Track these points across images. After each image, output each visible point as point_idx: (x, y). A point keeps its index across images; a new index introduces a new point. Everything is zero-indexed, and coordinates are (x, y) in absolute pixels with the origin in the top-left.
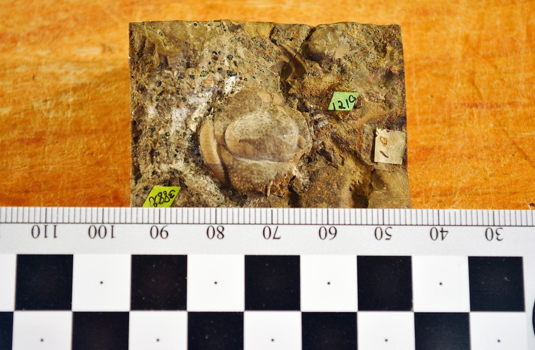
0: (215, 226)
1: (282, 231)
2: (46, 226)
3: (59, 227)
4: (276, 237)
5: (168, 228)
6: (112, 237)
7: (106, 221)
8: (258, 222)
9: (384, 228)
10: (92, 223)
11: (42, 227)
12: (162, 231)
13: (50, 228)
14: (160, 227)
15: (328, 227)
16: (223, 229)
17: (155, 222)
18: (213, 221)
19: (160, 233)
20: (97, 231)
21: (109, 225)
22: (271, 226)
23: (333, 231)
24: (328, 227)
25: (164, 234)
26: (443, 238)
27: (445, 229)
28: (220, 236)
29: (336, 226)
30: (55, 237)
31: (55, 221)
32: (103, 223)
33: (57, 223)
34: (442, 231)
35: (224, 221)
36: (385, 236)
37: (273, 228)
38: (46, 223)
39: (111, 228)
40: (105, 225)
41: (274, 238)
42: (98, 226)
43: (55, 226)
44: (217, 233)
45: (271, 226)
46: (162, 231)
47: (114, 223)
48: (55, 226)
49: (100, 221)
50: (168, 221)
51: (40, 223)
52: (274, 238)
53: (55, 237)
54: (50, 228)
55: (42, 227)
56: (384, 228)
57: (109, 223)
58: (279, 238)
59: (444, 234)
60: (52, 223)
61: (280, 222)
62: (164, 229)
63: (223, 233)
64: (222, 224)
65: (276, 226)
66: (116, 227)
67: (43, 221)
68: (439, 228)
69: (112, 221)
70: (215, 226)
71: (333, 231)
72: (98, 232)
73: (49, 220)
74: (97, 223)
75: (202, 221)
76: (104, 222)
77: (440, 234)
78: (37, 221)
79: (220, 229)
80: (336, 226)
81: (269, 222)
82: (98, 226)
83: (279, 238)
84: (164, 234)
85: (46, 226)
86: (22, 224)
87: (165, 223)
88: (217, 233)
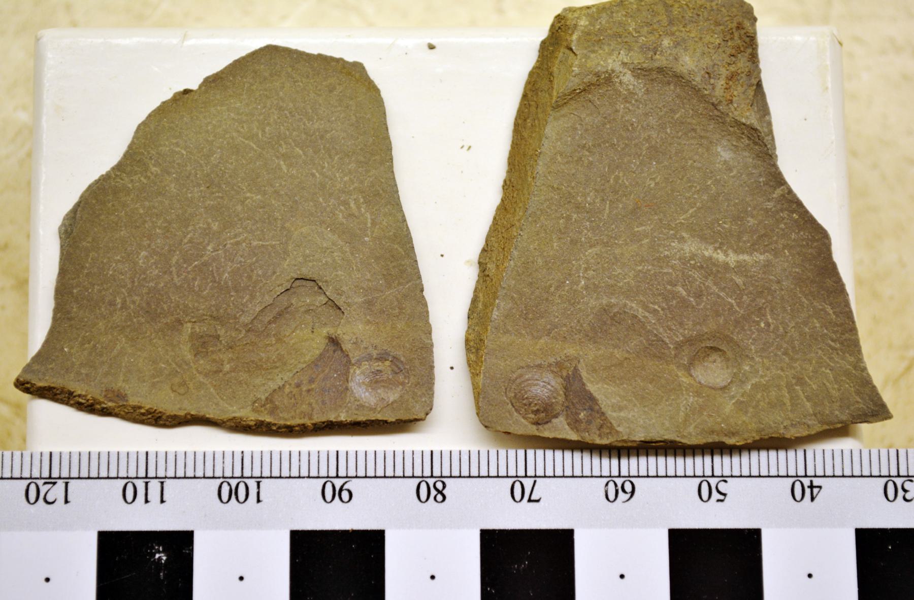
0: (431, 481)
1: (543, 488)
2: (147, 483)
3: (168, 483)
4: (532, 498)
5: (352, 485)
6: (259, 501)
7: (247, 473)
8: (503, 473)
9: (713, 482)
10: (224, 477)
11: (140, 484)
12: (341, 490)
13: (154, 486)
14: (338, 483)
16: (444, 487)
17: (330, 475)
18: (427, 473)
19: (338, 493)
21: (254, 480)
22: (524, 480)
23: (628, 487)
24: (619, 481)
25: (345, 495)
26: (813, 499)
27: (816, 482)
28: (440, 498)
29: (632, 479)
30: (162, 501)
31: (161, 474)
32: (242, 477)
33: (166, 477)
34: (812, 487)
35: (446, 473)
36: (716, 496)
37: (528, 483)
38: (146, 477)
39: (256, 484)
40: (246, 481)
41: (530, 500)
43: (162, 483)
44: (433, 492)
45: (524, 480)
46: (341, 490)
47: (261, 477)
48: (162, 483)
49: (238, 473)
50: (352, 473)
51: (137, 478)
52: (530, 500)
53: (162, 501)
54: (154, 486)
55: (140, 484)
56: (713, 482)
57: (252, 477)
58: (538, 501)
59: (815, 490)
60: (156, 478)
61: (540, 472)
62: (345, 487)
63: (444, 492)
64: (441, 477)
65: (532, 480)
66: (265, 483)
67: (142, 474)
68: (806, 482)
69: (257, 473)
70: (431, 481)
71: (628, 487)
72: (234, 493)
73: (151, 474)
74: (232, 477)
75: (408, 473)
76: (245, 475)
77: (808, 491)
78: (132, 474)
79: (439, 486)
80: (632, 479)
81: (521, 473)
82: (234, 483)
83: (538, 501)
84: (345, 495)
85: (147, 483)
86: (203, 480)
87: (347, 477)
88: (433, 492)
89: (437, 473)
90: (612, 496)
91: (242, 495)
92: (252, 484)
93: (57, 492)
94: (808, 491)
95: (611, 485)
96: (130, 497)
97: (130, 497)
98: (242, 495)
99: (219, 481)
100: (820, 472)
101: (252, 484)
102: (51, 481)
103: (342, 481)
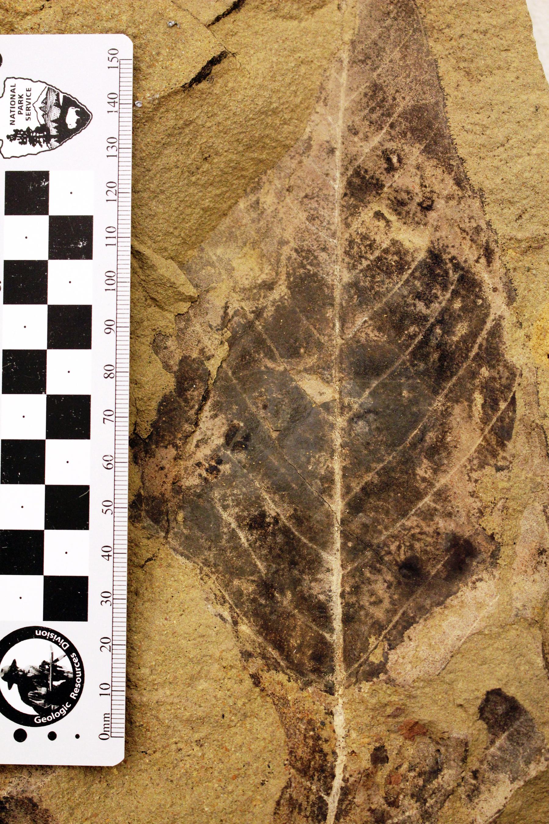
0: (114, 372)
1: (110, 425)
5: (113, 334)
7: (119, 284)
9: (112, 508)
11: (115, 234)
13: (114, 241)
14: (114, 327)
15: (113, 462)
19: (109, 327)
20: (111, 277)
22: (114, 416)
23: (110, 466)
24: (113, 462)
25: (108, 331)
28: (106, 376)
36: (105, 509)
37: (112, 418)
42: (115, 278)
44: (109, 373)
45: (114, 416)
54: (114, 241)
55: (115, 234)
56: (112, 508)
59: (107, 558)
67: (120, 235)
68: (111, 553)
69: (119, 289)
70: (114, 372)
71: (110, 466)
77: (107, 554)
79: (112, 376)
82: (115, 278)
84: (108, 331)
88: (109, 373)
89: (118, 374)
90: (106, 458)
91: (108, 282)
92: (114, 287)
93: (112, 196)
94: (107, 554)
95: (111, 458)
96: (109, 230)
97: (109, 230)
98: (108, 282)
99: (116, 271)
100: (115, 560)
101: (114, 287)
102: (117, 193)
103: (115, 329)
